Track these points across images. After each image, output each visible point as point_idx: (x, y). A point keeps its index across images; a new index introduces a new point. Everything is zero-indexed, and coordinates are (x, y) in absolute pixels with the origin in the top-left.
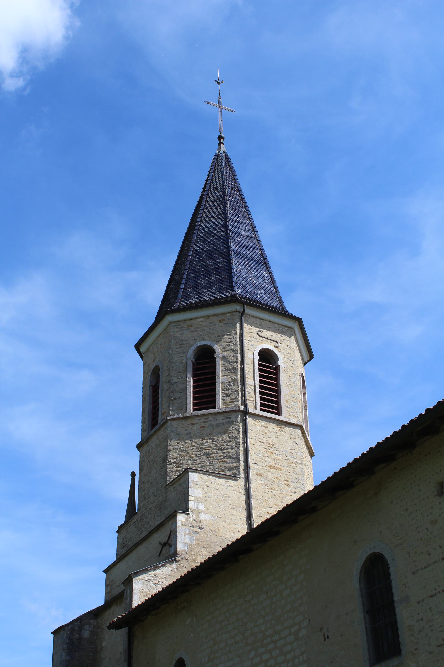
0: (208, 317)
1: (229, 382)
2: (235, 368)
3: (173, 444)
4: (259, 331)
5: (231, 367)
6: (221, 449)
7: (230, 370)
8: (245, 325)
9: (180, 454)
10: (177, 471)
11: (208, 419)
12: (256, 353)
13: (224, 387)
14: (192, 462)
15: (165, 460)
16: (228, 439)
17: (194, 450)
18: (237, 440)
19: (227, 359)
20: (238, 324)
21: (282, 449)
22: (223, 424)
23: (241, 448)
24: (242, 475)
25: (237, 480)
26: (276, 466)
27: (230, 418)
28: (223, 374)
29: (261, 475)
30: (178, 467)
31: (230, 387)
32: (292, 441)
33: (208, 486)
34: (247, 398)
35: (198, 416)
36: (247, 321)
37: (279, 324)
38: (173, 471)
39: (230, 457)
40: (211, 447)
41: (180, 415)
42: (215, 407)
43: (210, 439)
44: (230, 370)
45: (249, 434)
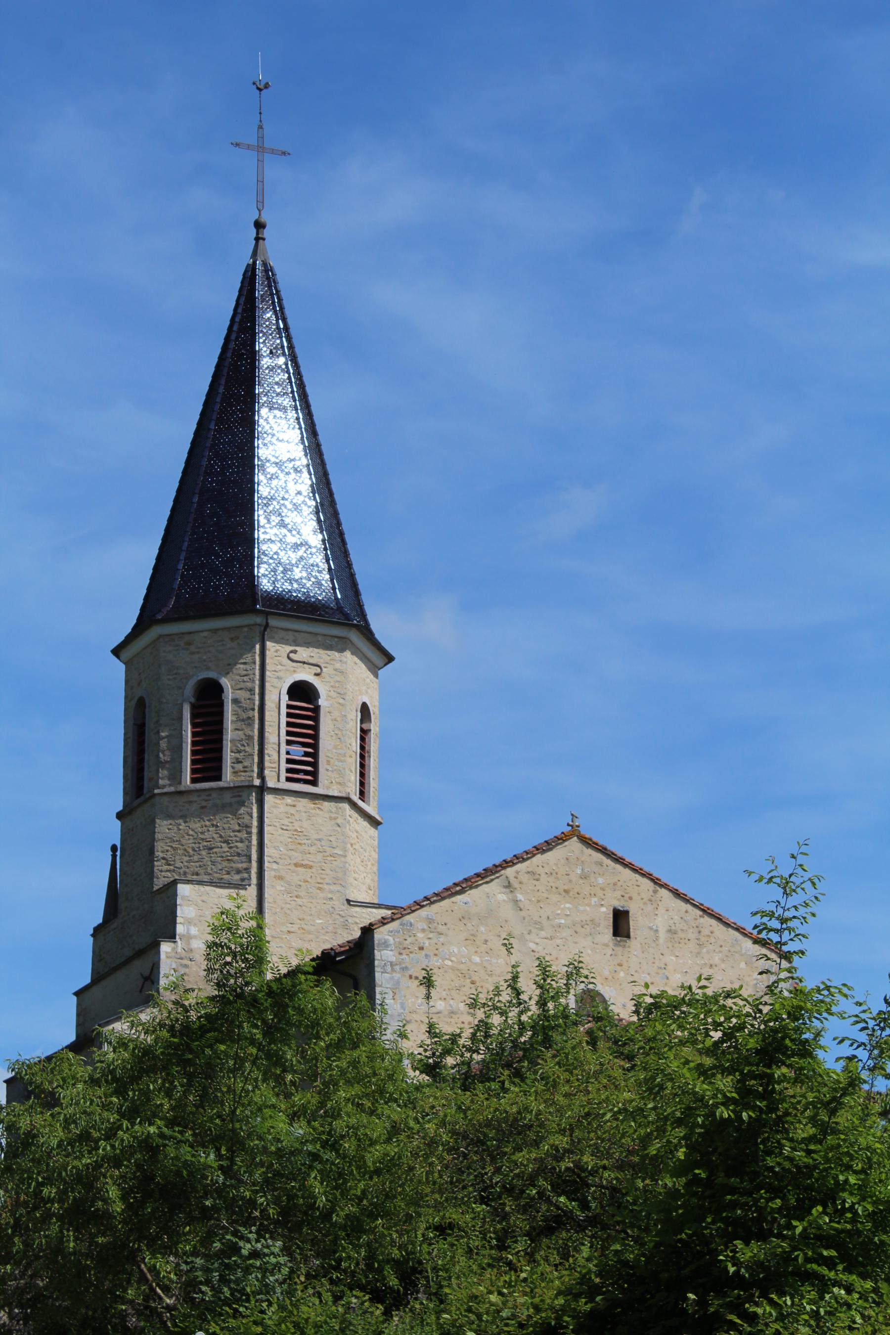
0: (215, 631)
1: (242, 740)
2: (250, 719)
3: (163, 827)
5: (245, 716)
6: (227, 842)
7: (243, 720)
8: (269, 644)
9: (171, 847)
10: (167, 871)
11: (210, 795)
12: (285, 691)
13: (234, 748)
14: (188, 858)
15: (152, 851)
16: (237, 828)
17: (191, 841)
18: (249, 830)
19: (240, 702)
20: (258, 647)
21: (316, 836)
22: (231, 804)
23: (254, 841)
24: (254, 880)
25: (246, 889)
26: (304, 863)
27: (240, 796)
28: (235, 726)
29: (281, 878)
30: (169, 865)
31: (243, 748)
32: (333, 822)
33: (203, 901)
34: (267, 764)
35: (197, 791)
36: (273, 638)
38: (161, 871)
39: (239, 855)
40: (213, 838)
41: (172, 789)
42: (219, 778)
43: (213, 825)
44: (243, 720)
45: (266, 820)
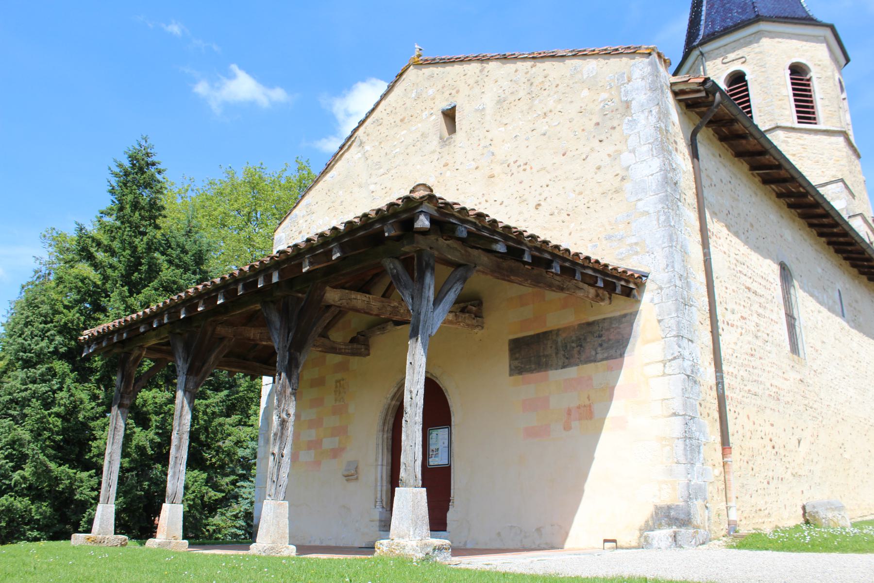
4: (723, 59)
20: (702, 67)
37: (744, 38)
